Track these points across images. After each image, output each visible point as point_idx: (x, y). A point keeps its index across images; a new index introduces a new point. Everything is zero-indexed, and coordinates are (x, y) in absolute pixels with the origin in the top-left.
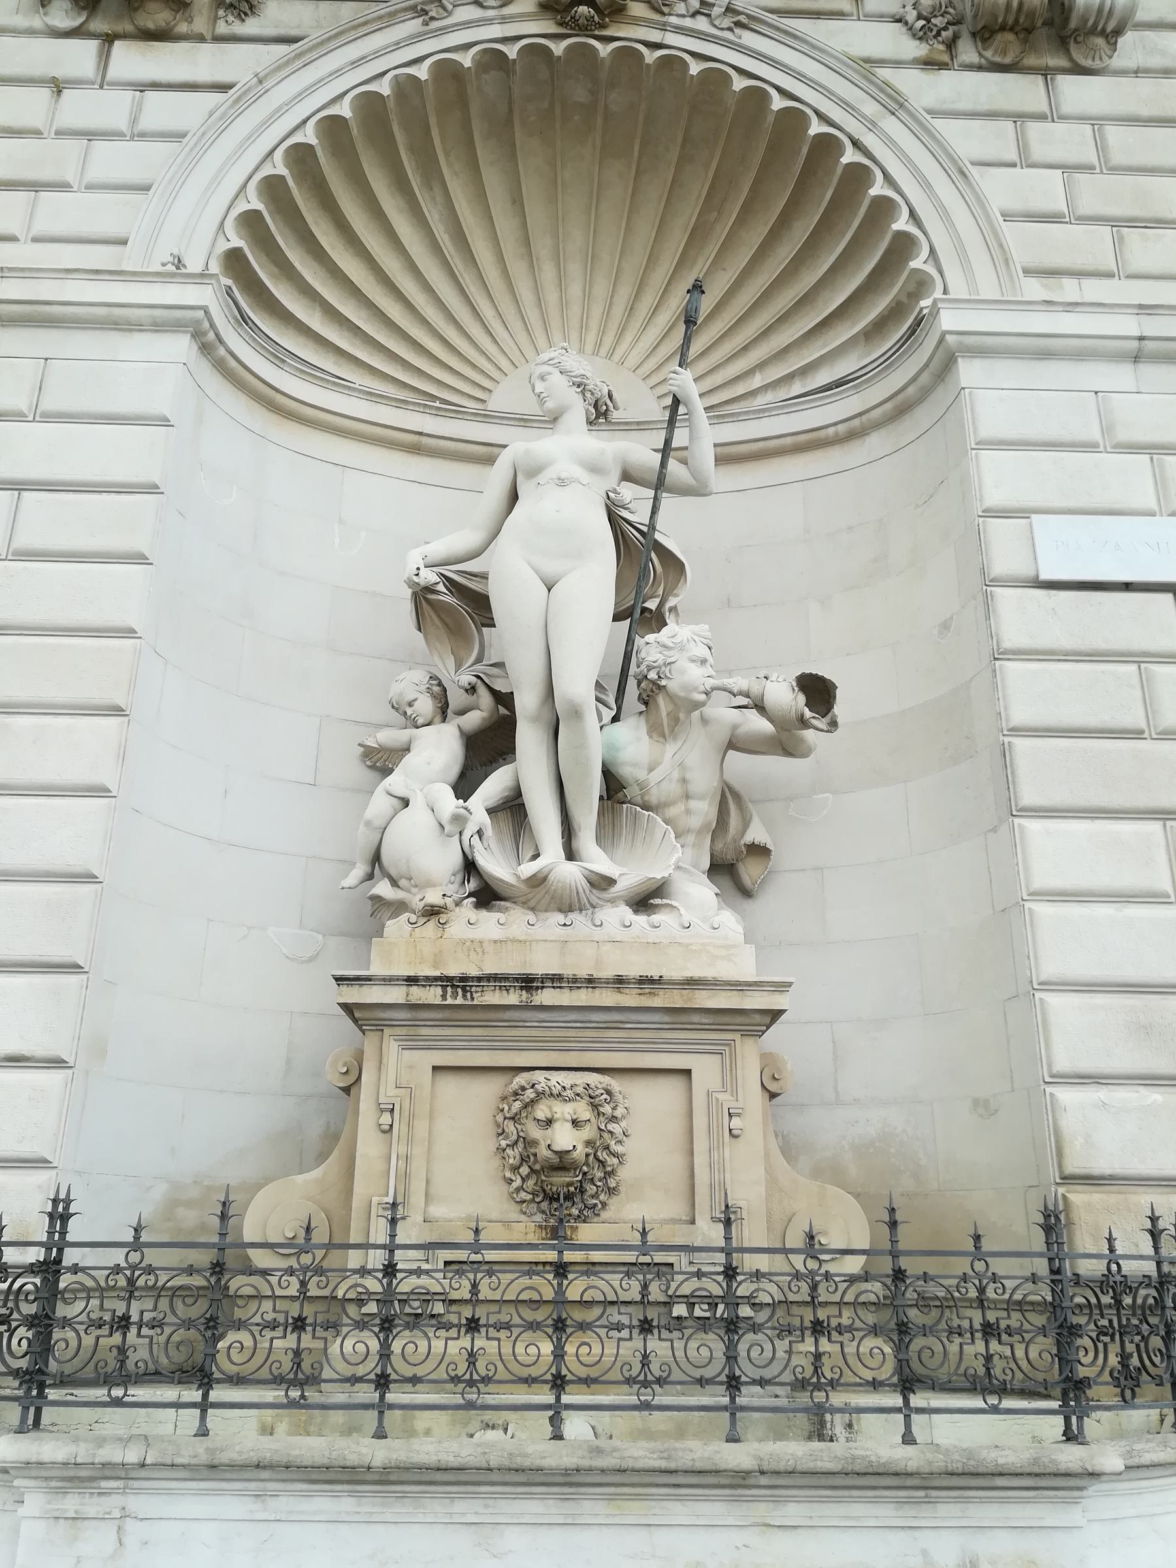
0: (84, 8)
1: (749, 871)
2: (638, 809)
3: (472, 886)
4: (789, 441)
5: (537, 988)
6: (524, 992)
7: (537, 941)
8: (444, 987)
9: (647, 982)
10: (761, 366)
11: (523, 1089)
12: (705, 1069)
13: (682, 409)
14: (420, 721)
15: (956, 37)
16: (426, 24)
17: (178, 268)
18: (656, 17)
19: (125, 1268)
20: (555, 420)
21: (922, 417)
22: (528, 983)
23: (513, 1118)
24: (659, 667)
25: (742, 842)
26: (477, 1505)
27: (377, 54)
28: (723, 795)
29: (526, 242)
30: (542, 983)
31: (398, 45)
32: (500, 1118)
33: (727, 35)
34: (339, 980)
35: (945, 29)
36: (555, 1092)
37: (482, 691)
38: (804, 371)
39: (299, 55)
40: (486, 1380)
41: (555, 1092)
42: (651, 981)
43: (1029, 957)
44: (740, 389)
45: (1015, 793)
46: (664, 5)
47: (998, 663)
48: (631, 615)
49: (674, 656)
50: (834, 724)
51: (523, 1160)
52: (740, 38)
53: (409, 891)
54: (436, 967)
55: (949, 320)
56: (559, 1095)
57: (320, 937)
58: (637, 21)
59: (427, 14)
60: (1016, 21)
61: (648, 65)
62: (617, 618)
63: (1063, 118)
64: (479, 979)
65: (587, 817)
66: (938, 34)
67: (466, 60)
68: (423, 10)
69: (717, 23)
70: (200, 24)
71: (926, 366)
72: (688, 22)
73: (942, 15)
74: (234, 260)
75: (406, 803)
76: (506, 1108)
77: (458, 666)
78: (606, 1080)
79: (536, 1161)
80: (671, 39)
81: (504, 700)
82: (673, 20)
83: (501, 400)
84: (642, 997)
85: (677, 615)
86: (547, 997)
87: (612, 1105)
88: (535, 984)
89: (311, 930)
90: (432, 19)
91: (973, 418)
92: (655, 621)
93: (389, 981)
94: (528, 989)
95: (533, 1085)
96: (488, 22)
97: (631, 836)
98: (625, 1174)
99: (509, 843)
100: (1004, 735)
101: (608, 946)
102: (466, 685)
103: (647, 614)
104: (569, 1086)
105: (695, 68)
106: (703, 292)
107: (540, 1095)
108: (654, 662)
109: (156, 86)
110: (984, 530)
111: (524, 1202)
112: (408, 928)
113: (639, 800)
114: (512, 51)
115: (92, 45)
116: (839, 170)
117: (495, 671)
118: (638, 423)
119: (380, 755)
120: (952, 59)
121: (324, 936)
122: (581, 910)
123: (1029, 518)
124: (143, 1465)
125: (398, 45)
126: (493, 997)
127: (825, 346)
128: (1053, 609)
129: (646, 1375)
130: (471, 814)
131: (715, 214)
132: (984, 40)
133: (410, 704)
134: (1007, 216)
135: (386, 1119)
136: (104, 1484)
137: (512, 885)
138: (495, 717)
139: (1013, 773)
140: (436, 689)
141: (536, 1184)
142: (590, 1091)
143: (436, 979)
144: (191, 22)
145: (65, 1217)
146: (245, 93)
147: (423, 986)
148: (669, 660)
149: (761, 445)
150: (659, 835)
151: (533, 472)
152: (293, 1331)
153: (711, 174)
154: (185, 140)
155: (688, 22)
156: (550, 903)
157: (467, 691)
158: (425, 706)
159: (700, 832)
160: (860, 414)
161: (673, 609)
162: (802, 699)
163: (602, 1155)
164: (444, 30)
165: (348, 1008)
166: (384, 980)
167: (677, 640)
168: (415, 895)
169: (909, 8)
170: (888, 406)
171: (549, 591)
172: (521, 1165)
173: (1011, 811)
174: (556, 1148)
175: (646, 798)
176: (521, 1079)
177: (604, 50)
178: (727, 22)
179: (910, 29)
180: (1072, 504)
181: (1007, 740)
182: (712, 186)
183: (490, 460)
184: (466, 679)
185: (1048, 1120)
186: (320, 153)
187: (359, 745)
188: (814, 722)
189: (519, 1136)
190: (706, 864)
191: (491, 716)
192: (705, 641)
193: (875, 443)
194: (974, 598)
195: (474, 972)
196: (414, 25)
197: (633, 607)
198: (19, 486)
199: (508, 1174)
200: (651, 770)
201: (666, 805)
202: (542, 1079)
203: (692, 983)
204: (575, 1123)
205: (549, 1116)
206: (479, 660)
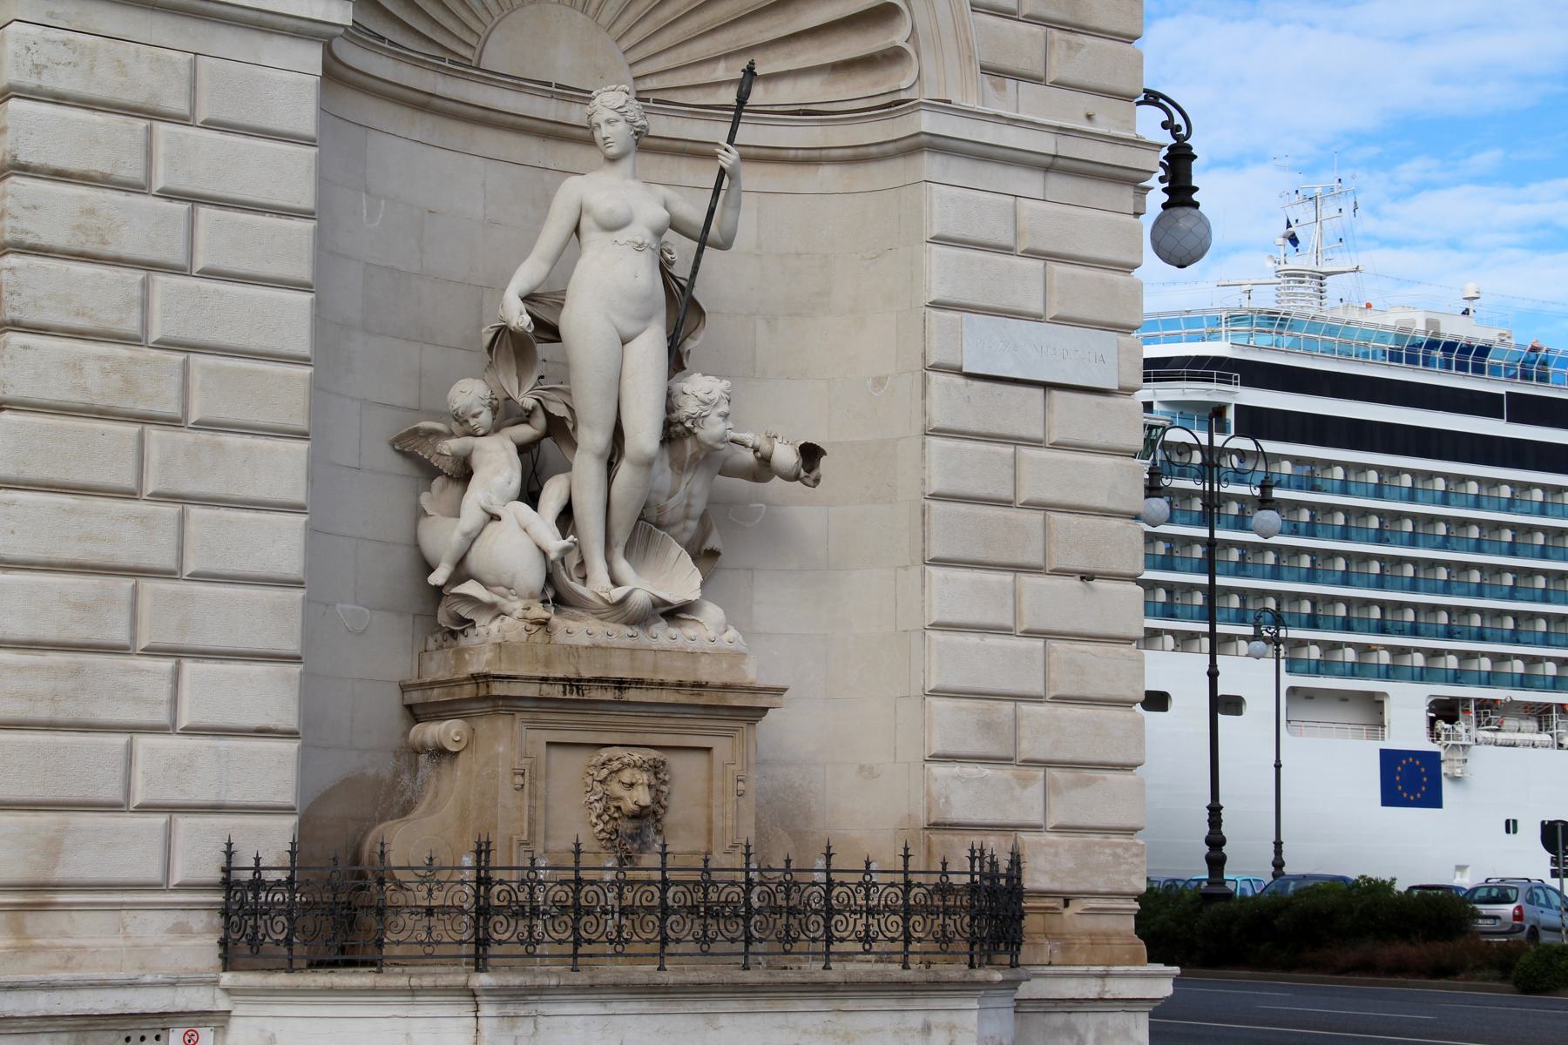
5: (625, 688)
6: (617, 691)
7: (615, 648)
8: (564, 686)
9: (698, 685)
12: (721, 746)
22: (621, 684)
23: (600, 782)
25: (704, 548)
26: (707, 1004)
32: (589, 780)
36: (639, 764)
41: (639, 764)
43: (924, 671)
56: (641, 767)
57: (367, 611)
64: (589, 680)
65: (621, 535)
71: (895, 141)
76: (596, 774)
84: (693, 697)
86: (632, 695)
89: (363, 606)
93: (528, 679)
94: (620, 689)
97: (643, 547)
101: (663, 653)
107: (625, 766)
108: (694, 414)
111: (603, 840)
124: (558, 986)
126: (596, 694)
135: (518, 779)
136: (529, 998)
141: (612, 827)
143: (561, 679)
147: (551, 684)
148: (704, 414)
166: (526, 679)
167: (711, 397)
171: (623, 344)
175: (660, 519)
176: (605, 754)
199: (594, 820)
201: (673, 524)
203: (726, 687)
205: (634, 781)
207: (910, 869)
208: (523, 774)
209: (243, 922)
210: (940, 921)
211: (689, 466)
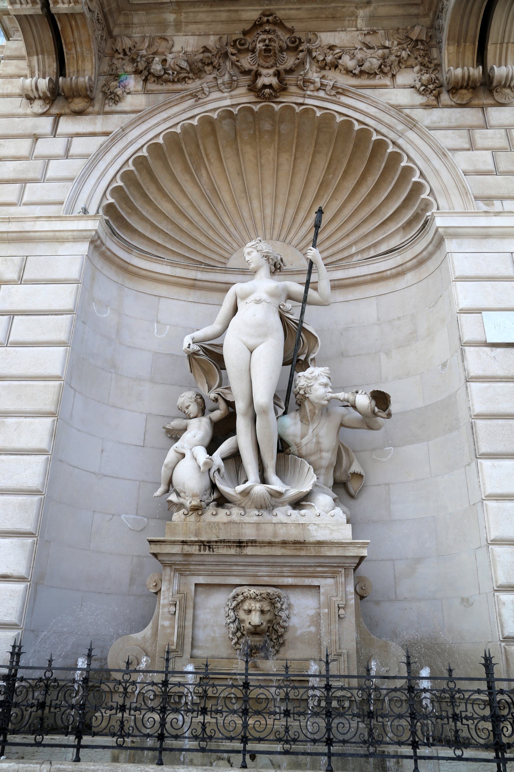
0: (48, 104)
1: (353, 486)
2: (296, 457)
3: (215, 495)
4: (369, 277)
5: (244, 546)
6: (238, 548)
7: (245, 523)
8: (200, 546)
10: (355, 243)
11: (238, 595)
13: (314, 266)
14: (192, 416)
15: (439, 93)
16: (196, 101)
17: (85, 213)
18: (302, 92)
19: (44, 680)
20: (255, 272)
21: (431, 265)
22: (240, 544)
24: (305, 388)
25: (349, 472)
27: (175, 115)
28: (339, 449)
29: (245, 191)
30: (247, 543)
31: (184, 111)
32: (227, 609)
33: (334, 98)
34: (151, 542)
35: (434, 90)
36: (253, 596)
37: (221, 401)
38: (375, 245)
39: (140, 118)
40: (211, 738)
41: (253, 596)
42: (300, 543)
44: (346, 254)
45: (478, 447)
46: (304, 86)
47: (468, 383)
48: (292, 363)
49: (313, 382)
50: (389, 415)
51: (238, 629)
52: (339, 99)
53: (185, 499)
54: (196, 535)
55: (439, 222)
56: (255, 598)
57: (146, 519)
58: (292, 94)
59: (197, 96)
60: (468, 84)
61: (297, 113)
62: (285, 364)
63: (492, 127)
64: (216, 542)
65: (270, 462)
66: (431, 92)
67: (215, 116)
68: (195, 95)
69: (328, 93)
70: (97, 108)
71: (431, 242)
72: (315, 94)
73: (433, 84)
74: (110, 209)
75: (183, 456)
77: (210, 389)
78: (278, 591)
79: (244, 630)
80: (308, 101)
81: (231, 405)
82: (309, 93)
83: (232, 263)
84: (295, 551)
85: (315, 362)
86: (249, 551)
87: (281, 603)
88: (243, 545)
89: (142, 516)
90: (199, 98)
91: (453, 266)
92: (304, 365)
93: (174, 542)
94: (240, 547)
95: (242, 594)
96: (225, 98)
98: (287, 636)
99: (233, 475)
100: (472, 418)
101: (280, 525)
102: (213, 398)
103: (300, 362)
104: (259, 594)
105: (318, 113)
106: (323, 213)
107: (245, 598)
108: (303, 386)
109: (78, 135)
110: (460, 319)
112: (183, 517)
113: (296, 452)
114: (235, 111)
115: (51, 119)
116: (387, 155)
117: (226, 391)
118: (297, 271)
119: (174, 432)
120: (438, 103)
121: (148, 519)
122: (267, 508)
123: (481, 313)
125: (184, 111)
127: (385, 233)
128: (494, 357)
129: (287, 737)
130: (213, 461)
131: (331, 176)
132: (453, 94)
133: (187, 408)
134: (466, 173)
135: (172, 609)
137: (234, 496)
138: (227, 413)
139: (476, 437)
140: (199, 400)
142: (270, 596)
144: (94, 107)
145: (19, 655)
146: (116, 136)
148: (310, 385)
149: (356, 280)
150: (306, 470)
151: (245, 297)
152: (120, 712)
153: (329, 158)
154: (90, 158)
155: (315, 94)
156: (251, 505)
157: (213, 401)
158: (193, 409)
159: (327, 468)
160: (402, 265)
161: (313, 359)
162: (373, 403)
163: (277, 627)
164: (205, 103)
165: (155, 555)
166: (171, 542)
167: (313, 375)
168: (187, 500)
169: (417, 82)
170: (414, 261)
171: (251, 353)
172: (237, 631)
173: (476, 455)
174: (252, 623)
175: (300, 452)
177: (277, 107)
178: (333, 92)
179: (418, 90)
180: (503, 306)
181: (473, 421)
182: (330, 163)
183: (226, 290)
184: (213, 395)
185: (496, 609)
186: (149, 159)
187: (163, 428)
188: (380, 414)
189: (236, 618)
190: (331, 482)
191: (225, 413)
192: (327, 375)
193: (409, 277)
194: (457, 351)
195: (214, 539)
196: (191, 102)
197: (293, 359)
198: (12, 314)
199: (231, 636)
200: (302, 438)
201: (311, 455)
202: (246, 590)
204: (262, 612)
205: (250, 608)
206: (220, 386)
208: (175, 605)
211: (312, 419)
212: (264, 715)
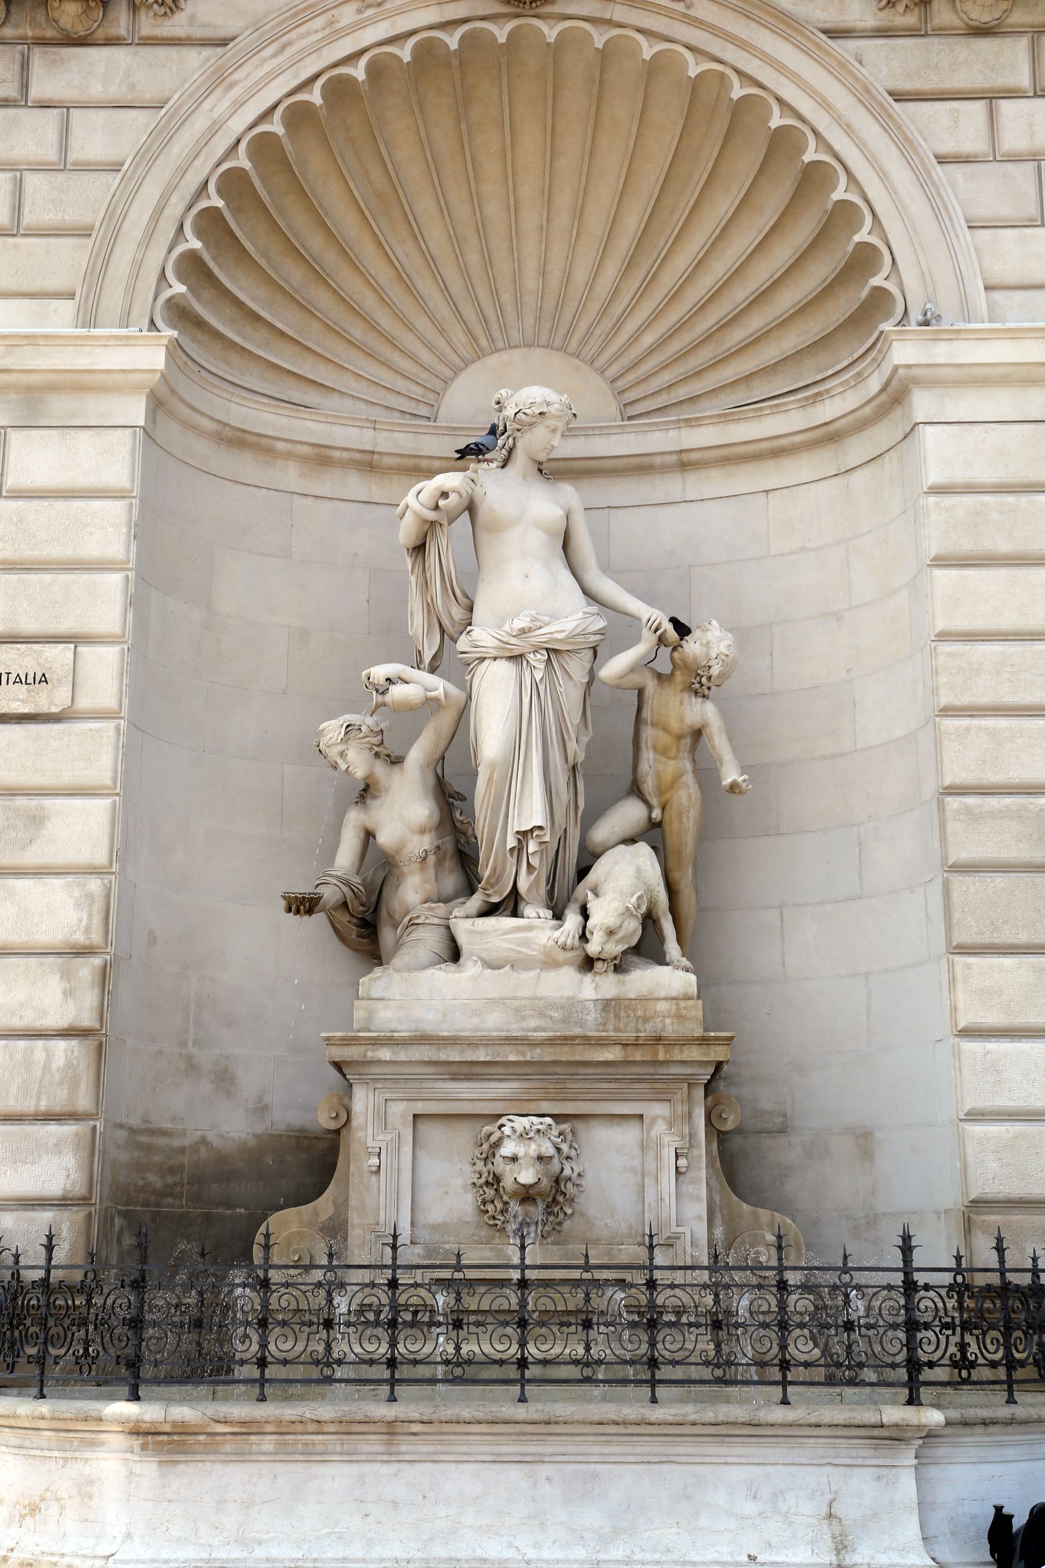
135: (375, 1161)
207: (1007, 1266)
209: (70, 1335)
210: (956, 1339)
212: (552, 1327)
